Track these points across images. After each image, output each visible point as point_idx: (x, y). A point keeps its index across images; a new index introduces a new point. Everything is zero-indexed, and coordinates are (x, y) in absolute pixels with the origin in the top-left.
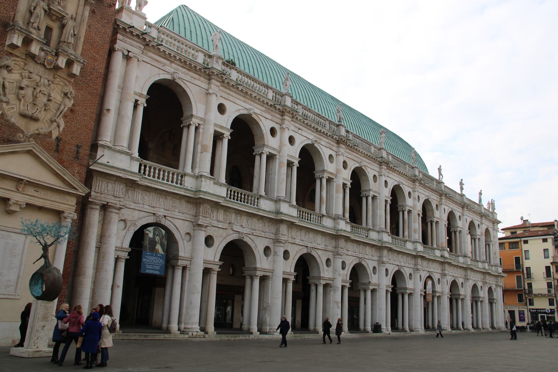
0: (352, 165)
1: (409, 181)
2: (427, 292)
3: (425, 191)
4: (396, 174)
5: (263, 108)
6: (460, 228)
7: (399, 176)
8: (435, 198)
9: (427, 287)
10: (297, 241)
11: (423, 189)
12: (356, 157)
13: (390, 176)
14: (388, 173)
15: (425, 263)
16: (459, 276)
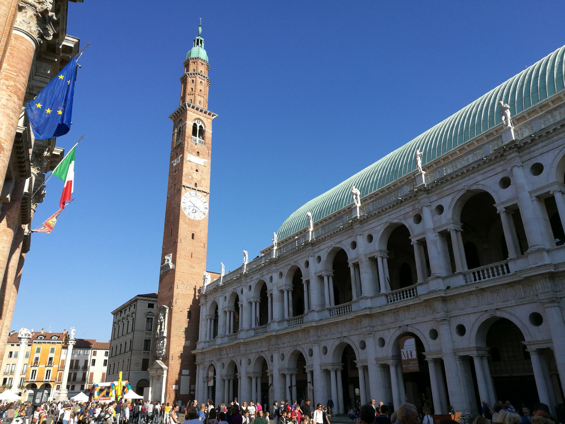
0: (285, 271)
1: (347, 233)
2: (403, 358)
3: (380, 220)
4: (327, 241)
5: (237, 283)
6: (503, 203)
7: (332, 239)
8: (411, 209)
9: (402, 350)
10: (253, 351)
11: (375, 220)
12: (287, 261)
13: (322, 247)
14: (318, 247)
15: (388, 319)
16: (513, 303)
